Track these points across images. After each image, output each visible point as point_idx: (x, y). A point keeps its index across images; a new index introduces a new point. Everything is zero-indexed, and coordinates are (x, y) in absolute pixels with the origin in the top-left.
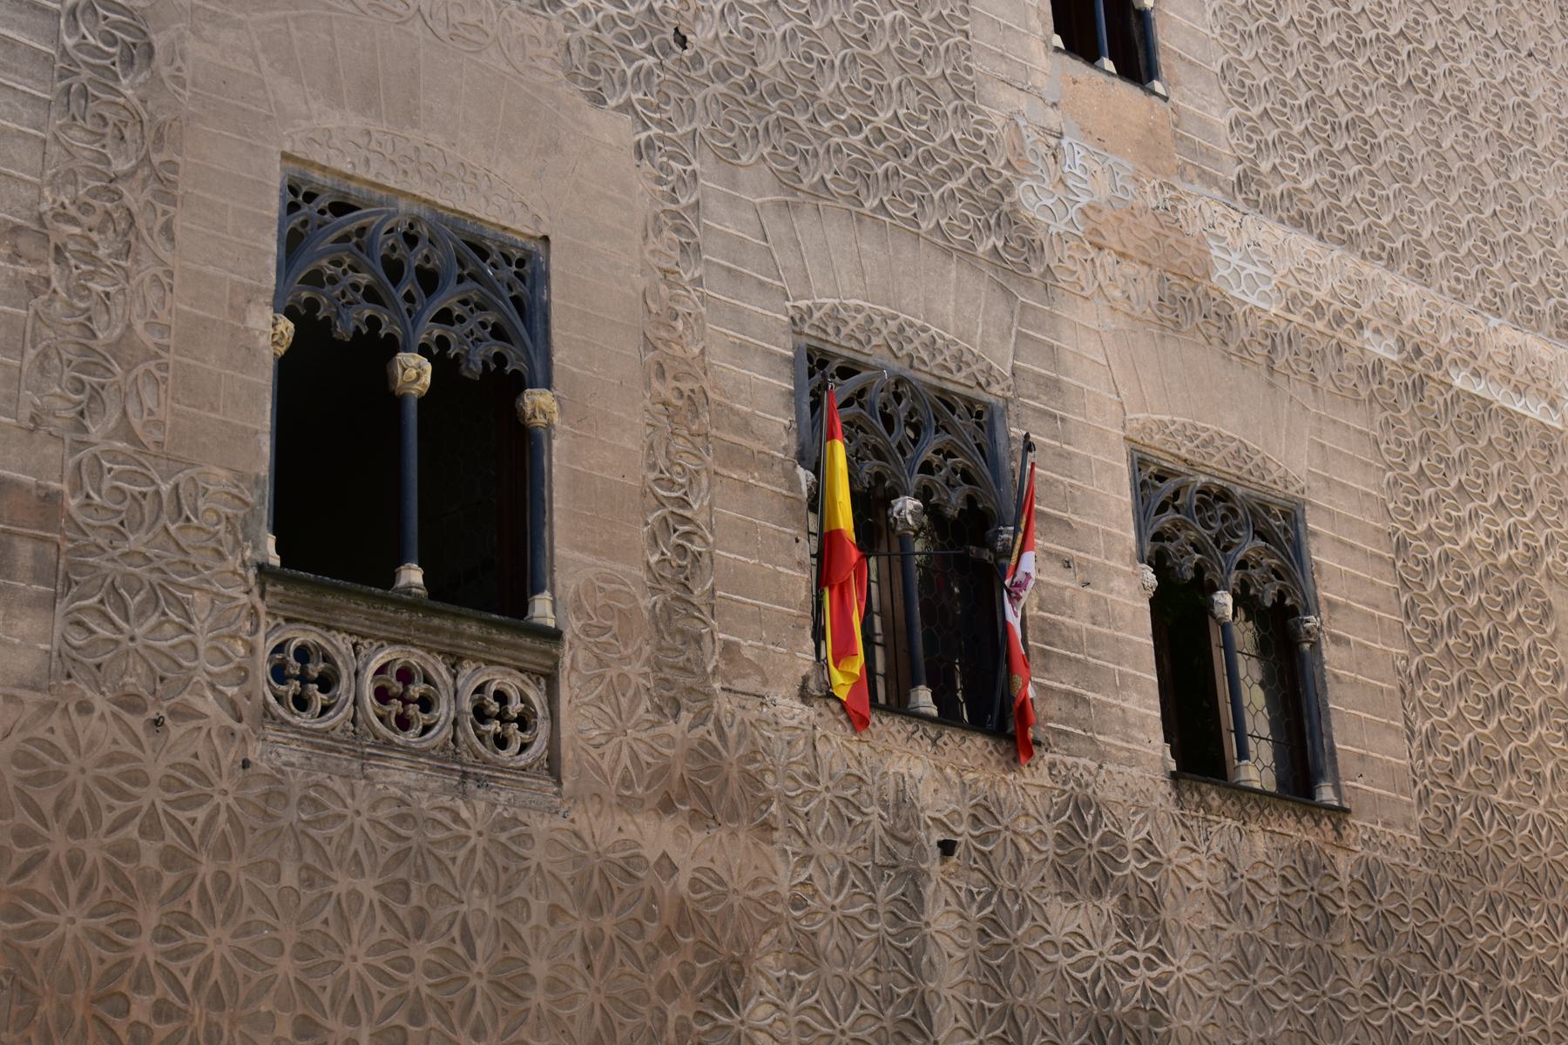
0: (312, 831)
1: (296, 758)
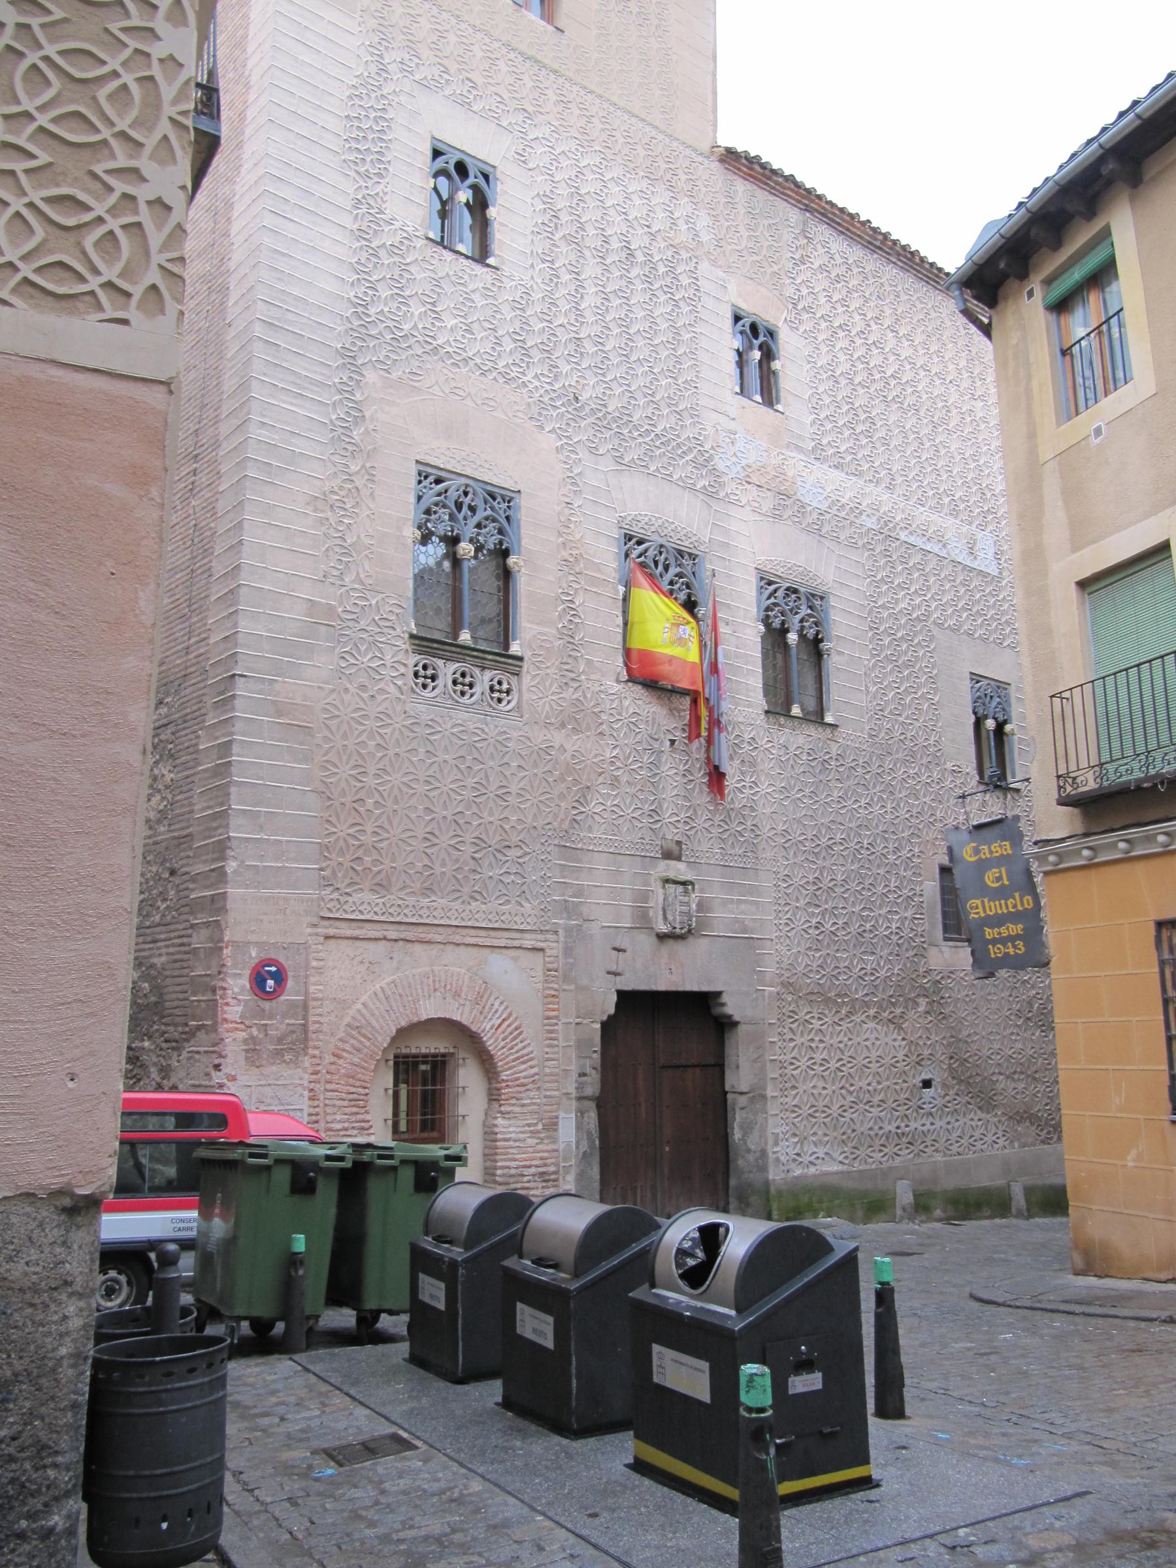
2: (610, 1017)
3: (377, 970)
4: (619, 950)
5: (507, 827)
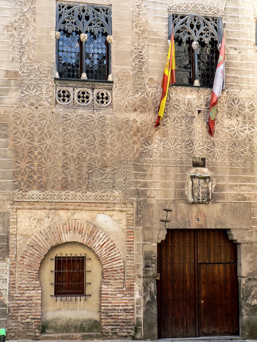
0: (64, 122)
1: (62, 110)
2: (162, 241)
3: (42, 222)
4: (168, 211)
5: (105, 158)
